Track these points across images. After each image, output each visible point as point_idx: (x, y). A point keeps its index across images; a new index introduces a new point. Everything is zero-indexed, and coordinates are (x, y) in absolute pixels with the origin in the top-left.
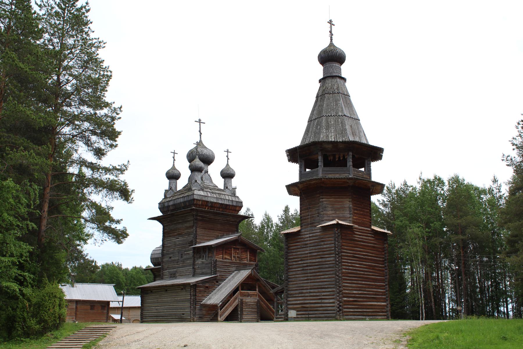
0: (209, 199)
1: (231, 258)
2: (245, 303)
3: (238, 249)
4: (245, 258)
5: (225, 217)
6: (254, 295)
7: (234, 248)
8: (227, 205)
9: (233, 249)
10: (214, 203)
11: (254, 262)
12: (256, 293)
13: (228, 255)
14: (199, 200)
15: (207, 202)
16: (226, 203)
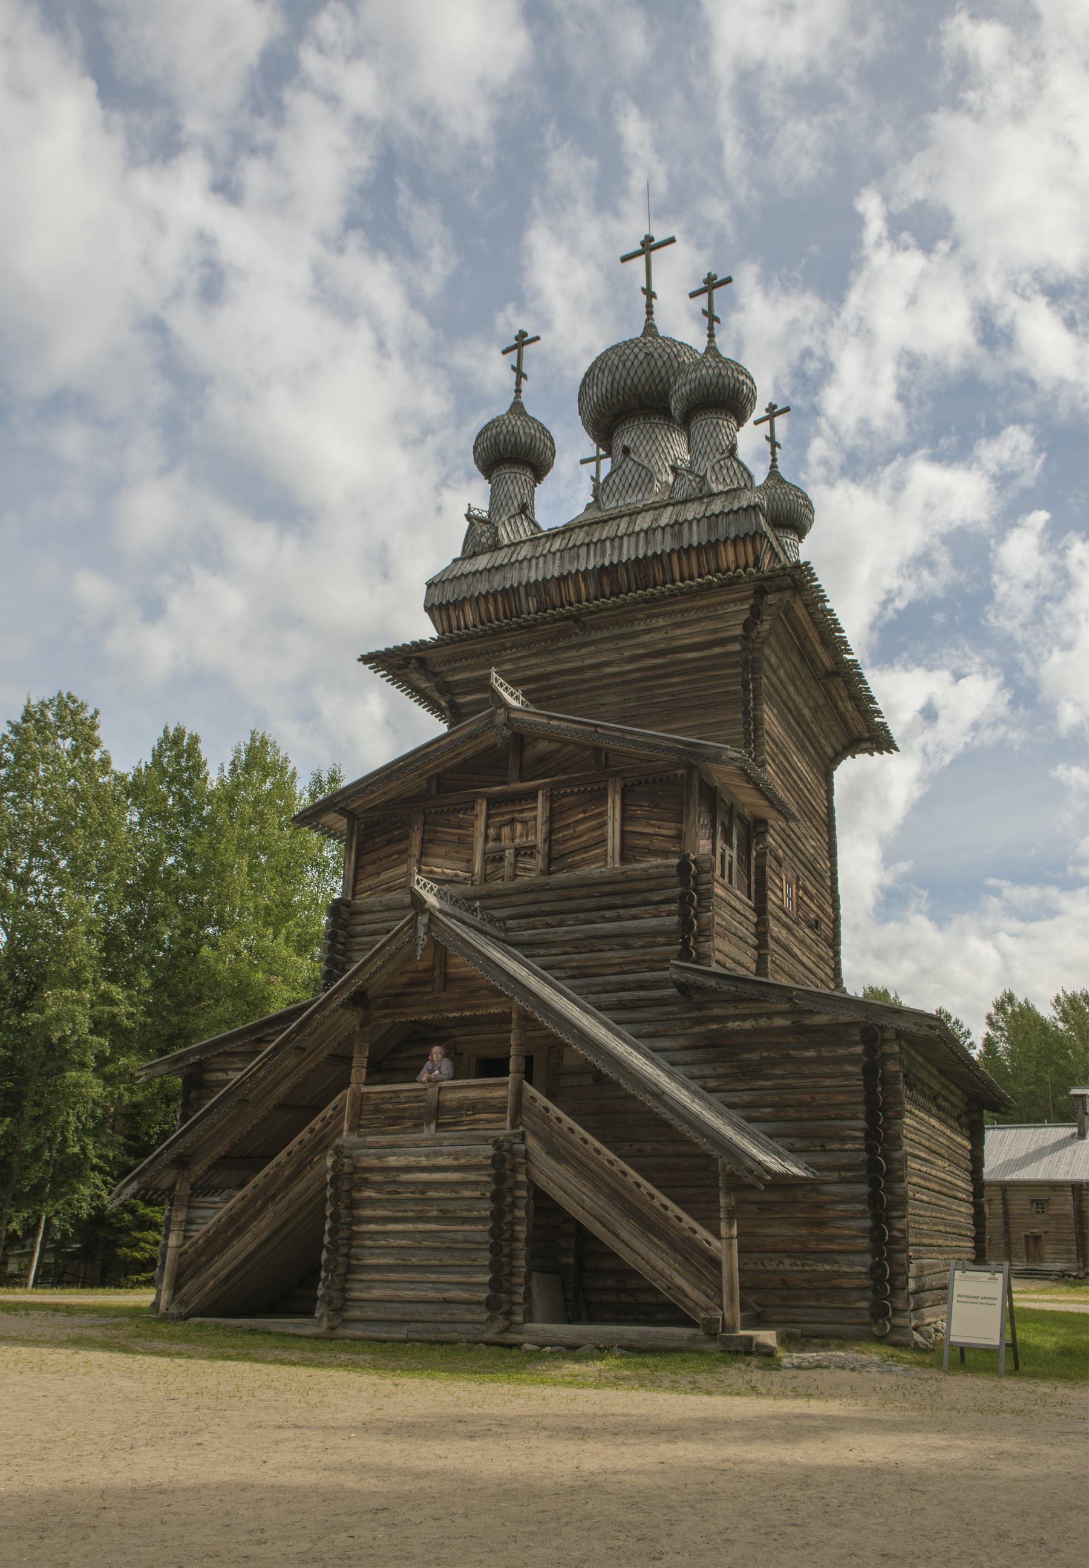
0: (513, 578)
1: (470, 870)
2: (377, 1177)
3: (530, 796)
4: (587, 848)
5: (622, 637)
6: (474, 1107)
7: (494, 802)
8: (640, 564)
9: (481, 808)
10: (553, 589)
11: (665, 853)
12: (500, 1093)
13: (446, 856)
14: (458, 604)
15: (507, 593)
16: (629, 552)
